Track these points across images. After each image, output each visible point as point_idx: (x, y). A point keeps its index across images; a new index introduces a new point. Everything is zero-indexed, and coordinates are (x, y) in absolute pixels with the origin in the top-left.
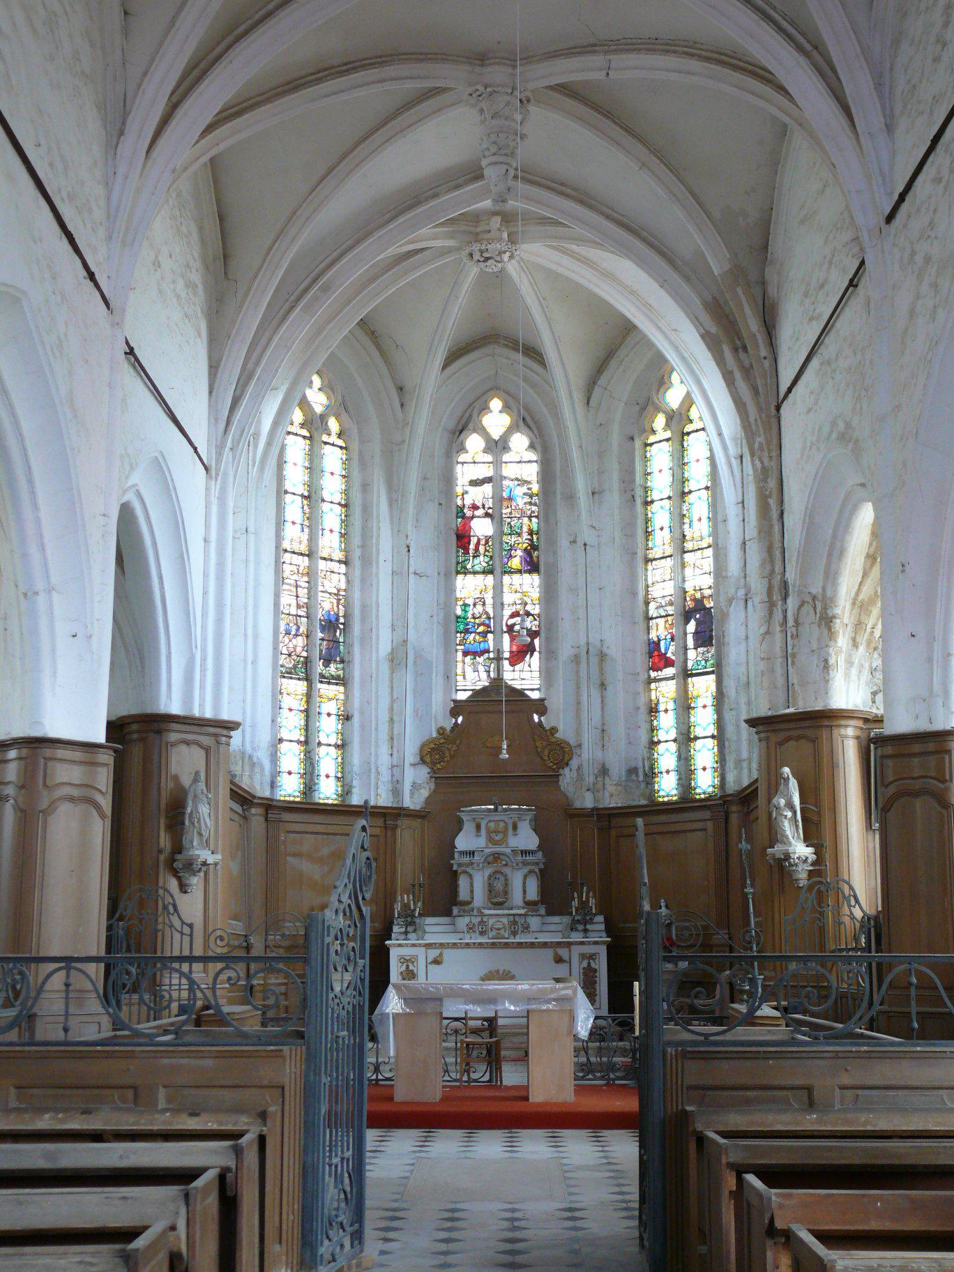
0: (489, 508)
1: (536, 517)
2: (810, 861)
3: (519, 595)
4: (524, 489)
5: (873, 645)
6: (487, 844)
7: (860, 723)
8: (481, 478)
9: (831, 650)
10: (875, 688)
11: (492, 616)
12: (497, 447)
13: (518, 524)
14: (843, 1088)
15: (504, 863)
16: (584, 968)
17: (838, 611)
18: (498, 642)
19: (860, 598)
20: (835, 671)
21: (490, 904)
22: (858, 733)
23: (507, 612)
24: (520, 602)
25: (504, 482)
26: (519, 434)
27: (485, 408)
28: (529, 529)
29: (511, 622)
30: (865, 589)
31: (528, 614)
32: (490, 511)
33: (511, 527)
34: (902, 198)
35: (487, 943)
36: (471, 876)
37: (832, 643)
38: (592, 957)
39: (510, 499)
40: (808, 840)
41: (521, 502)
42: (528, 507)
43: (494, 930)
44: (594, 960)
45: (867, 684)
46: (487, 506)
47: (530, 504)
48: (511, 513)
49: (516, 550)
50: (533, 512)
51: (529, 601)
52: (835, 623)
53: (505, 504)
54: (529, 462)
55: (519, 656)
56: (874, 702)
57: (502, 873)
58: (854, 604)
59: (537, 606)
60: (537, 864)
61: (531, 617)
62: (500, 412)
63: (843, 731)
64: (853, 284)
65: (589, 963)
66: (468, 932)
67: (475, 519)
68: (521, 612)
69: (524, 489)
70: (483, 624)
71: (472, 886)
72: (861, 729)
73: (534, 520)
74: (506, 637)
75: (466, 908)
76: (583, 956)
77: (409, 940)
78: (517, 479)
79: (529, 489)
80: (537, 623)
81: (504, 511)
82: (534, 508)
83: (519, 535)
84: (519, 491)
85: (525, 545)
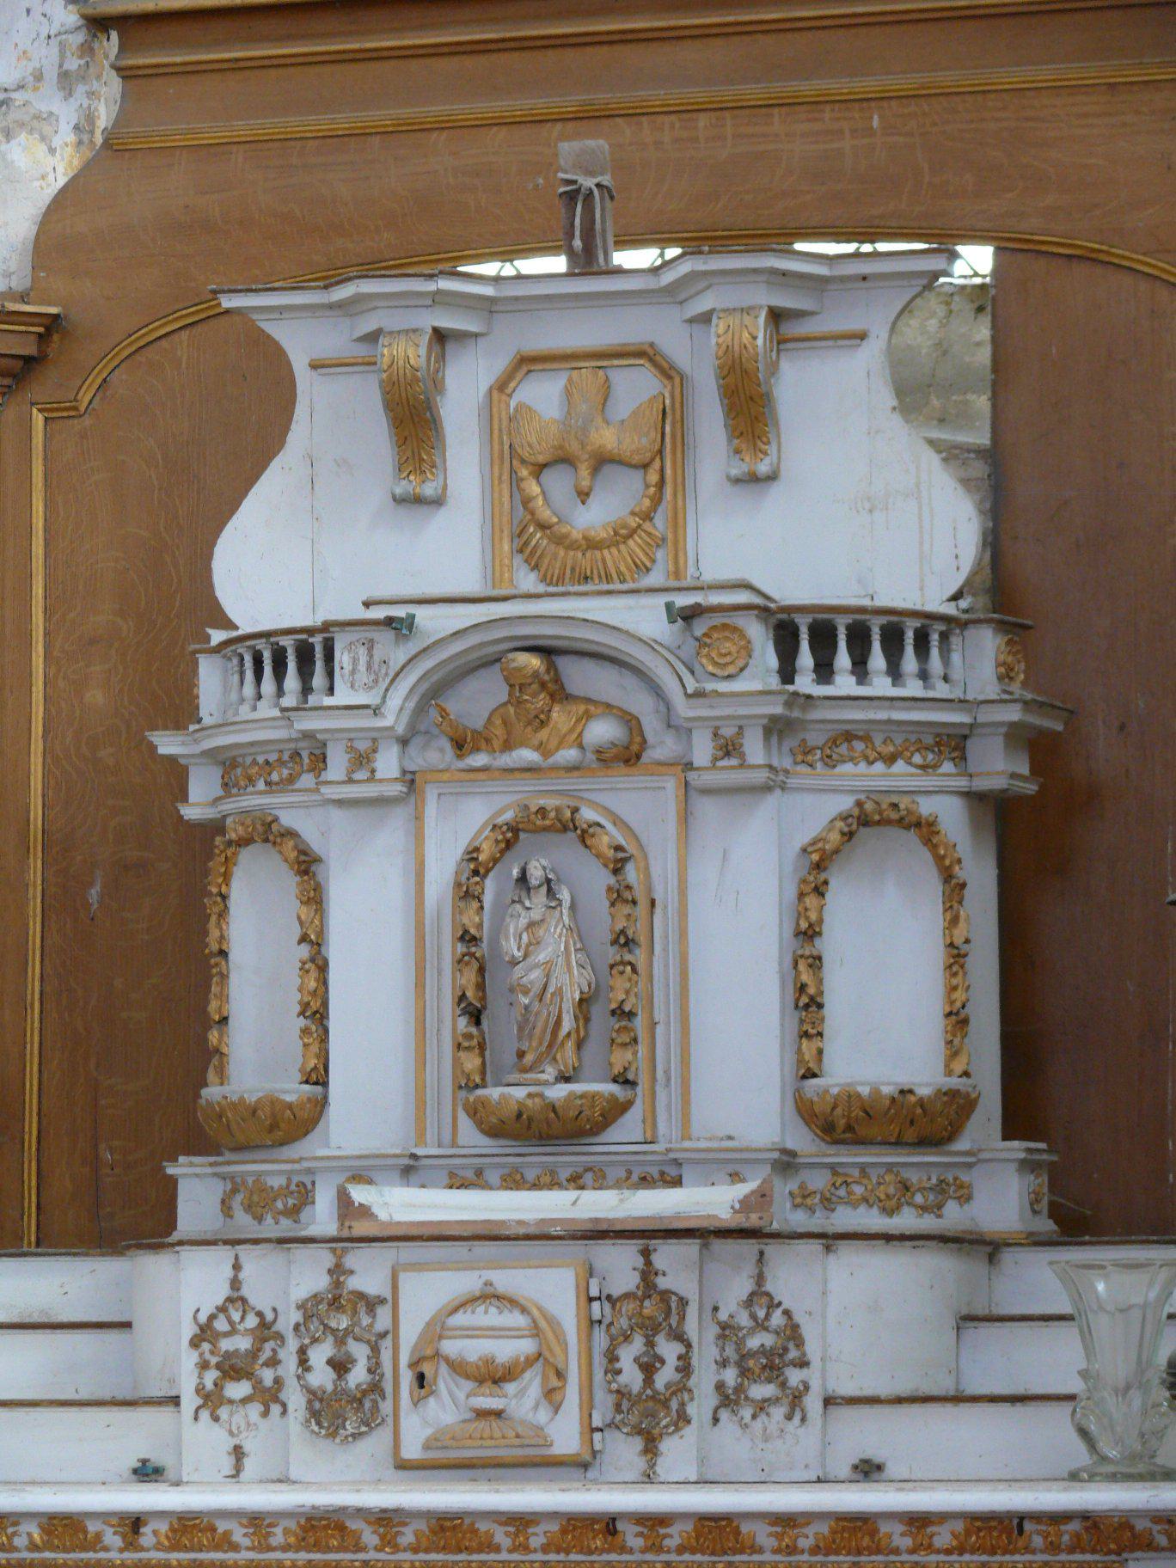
6: (495, 569)
15: (602, 731)
21: (470, 1135)
35: (387, 1520)
36: (306, 865)
43: (444, 1381)
57: (585, 836)
66: (211, 1400)
71: (314, 943)
75: (271, 1170)
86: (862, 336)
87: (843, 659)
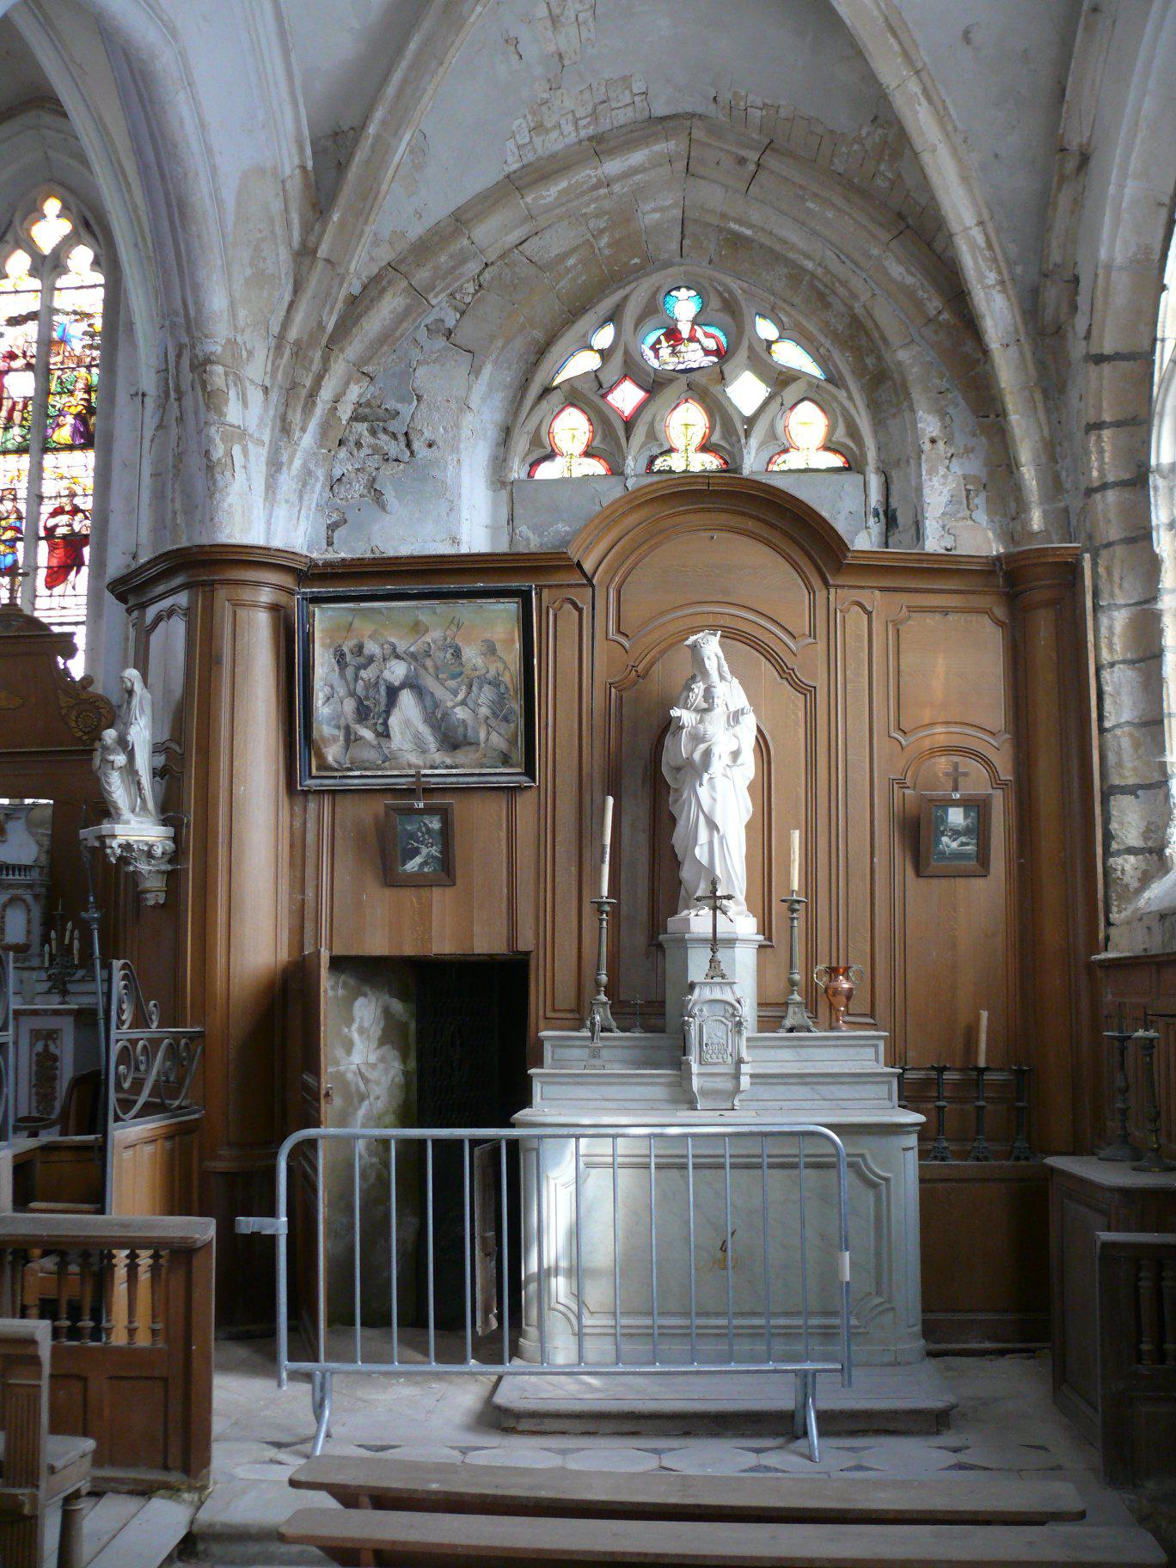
0: (31, 357)
1: (96, 366)
2: (158, 851)
3: (65, 483)
4: (83, 326)
8: (24, 313)
9: (213, 429)
10: (335, 517)
11: (24, 515)
12: (49, 266)
13: (72, 379)
16: (38, 1054)
18: (31, 553)
20: (228, 474)
23: (47, 508)
24: (66, 492)
25: (55, 318)
26: (81, 247)
27: (36, 213)
28: (86, 385)
29: (51, 522)
30: (299, 318)
31: (75, 510)
32: (33, 361)
33: (62, 383)
37: (213, 417)
38: (51, 1035)
39: (63, 341)
40: (169, 812)
41: (77, 346)
42: (88, 352)
44: (54, 1040)
46: (29, 354)
47: (91, 347)
48: (62, 363)
49: (64, 416)
50: (94, 359)
51: (79, 491)
52: (211, 373)
53: (54, 349)
54: (95, 286)
55: (56, 576)
56: (330, 543)
59: (90, 499)
60: (30, 886)
61: (80, 515)
62: (58, 216)
63: (246, 594)
65: (46, 1046)
67: (11, 374)
68: (68, 508)
69: (83, 326)
70: (11, 528)
73: (95, 371)
74: (43, 546)
76: (36, 1034)
77: (68, 1003)
78: (75, 313)
79: (90, 325)
80: (88, 523)
81: (52, 360)
82: (96, 353)
83: (71, 393)
84: (76, 330)
85: (80, 408)
86: (19, 818)
87: (11, 872)
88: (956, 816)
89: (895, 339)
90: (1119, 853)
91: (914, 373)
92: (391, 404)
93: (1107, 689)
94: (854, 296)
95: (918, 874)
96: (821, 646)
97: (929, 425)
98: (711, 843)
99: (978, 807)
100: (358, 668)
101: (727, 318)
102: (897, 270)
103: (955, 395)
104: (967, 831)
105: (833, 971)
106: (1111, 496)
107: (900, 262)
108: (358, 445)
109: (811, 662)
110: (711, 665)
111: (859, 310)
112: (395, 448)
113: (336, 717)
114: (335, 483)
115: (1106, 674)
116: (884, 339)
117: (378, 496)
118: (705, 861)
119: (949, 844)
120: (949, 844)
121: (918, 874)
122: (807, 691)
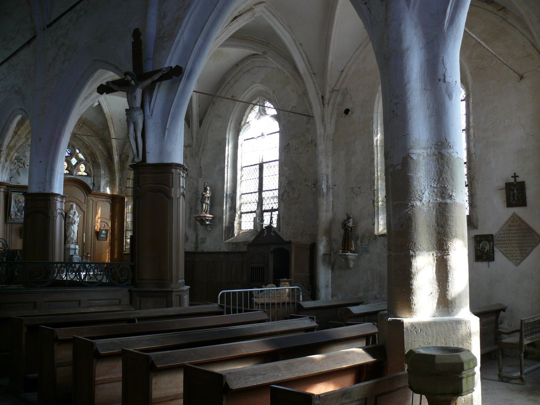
5: (12, 162)
7: (5, 187)
10: (11, 176)
14: (45, 302)
17: (3, 149)
19: (10, 145)
22: (5, 190)
34: (55, 21)
45: (8, 174)
56: (10, 180)
58: (7, 147)
64: (29, 43)
72: (6, 189)
88: (104, 232)
89: (99, 158)
90: (127, 239)
91: (101, 163)
92: (21, 158)
93: (127, 216)
94: (93, 149)
95: (98, 239)
96: (86, 205)
97: (102, 172)
98: (73, 235)
99: (107, 231)
100: (18, 203)
101: (72, 149)
102: (100, 147)
103: (107, 168)
104: (105, 234)
105: (87, 254)
106: (130, 189)
107: (101, 145)
108: (15, 164)
109: (84, 207)
110: (74, 208)
111: (93, 152)
112: (21, 165)
113: (14, 211)
114: (11, 170)
115: (127, 214)
116: (97, 157)
117: (19, 173)
118: (72, 237)
119: (102, 236)
120: (102, 236)
121: (98, 240)
122: (84, 212)
